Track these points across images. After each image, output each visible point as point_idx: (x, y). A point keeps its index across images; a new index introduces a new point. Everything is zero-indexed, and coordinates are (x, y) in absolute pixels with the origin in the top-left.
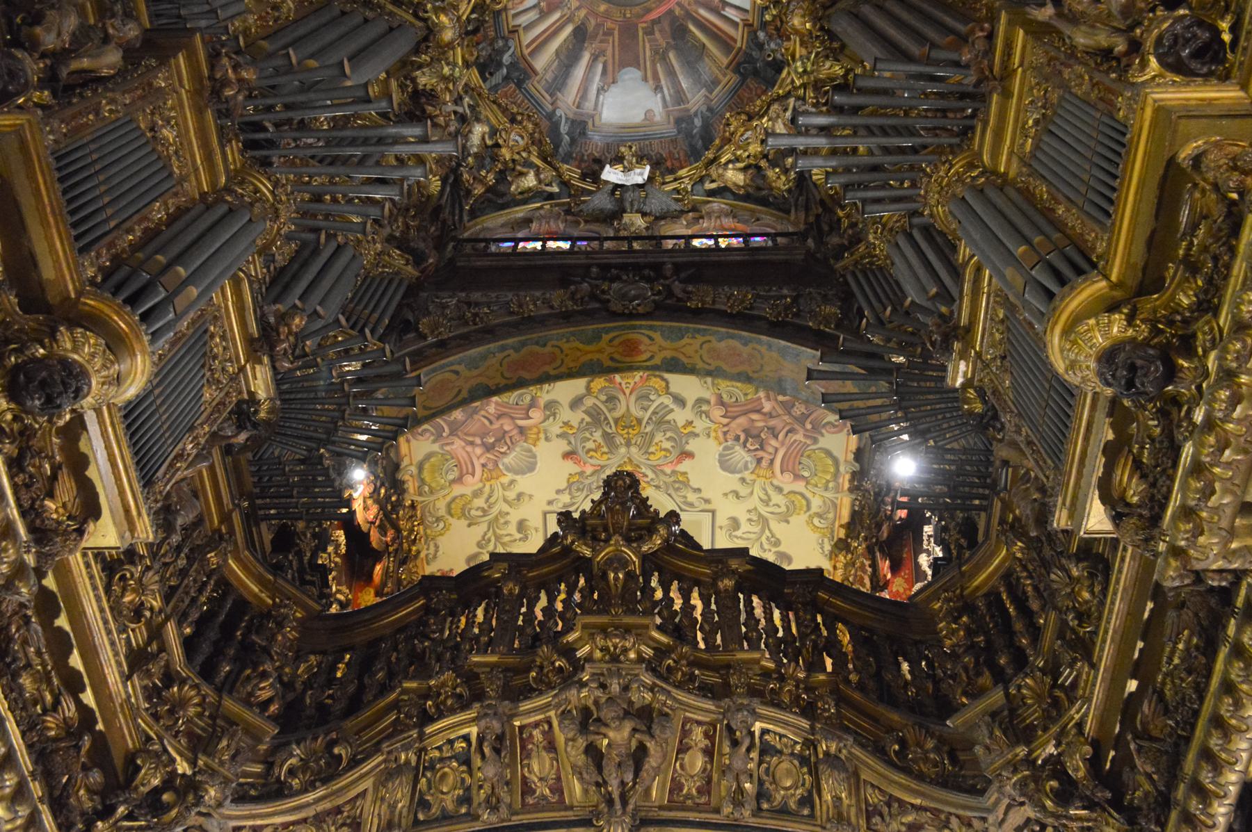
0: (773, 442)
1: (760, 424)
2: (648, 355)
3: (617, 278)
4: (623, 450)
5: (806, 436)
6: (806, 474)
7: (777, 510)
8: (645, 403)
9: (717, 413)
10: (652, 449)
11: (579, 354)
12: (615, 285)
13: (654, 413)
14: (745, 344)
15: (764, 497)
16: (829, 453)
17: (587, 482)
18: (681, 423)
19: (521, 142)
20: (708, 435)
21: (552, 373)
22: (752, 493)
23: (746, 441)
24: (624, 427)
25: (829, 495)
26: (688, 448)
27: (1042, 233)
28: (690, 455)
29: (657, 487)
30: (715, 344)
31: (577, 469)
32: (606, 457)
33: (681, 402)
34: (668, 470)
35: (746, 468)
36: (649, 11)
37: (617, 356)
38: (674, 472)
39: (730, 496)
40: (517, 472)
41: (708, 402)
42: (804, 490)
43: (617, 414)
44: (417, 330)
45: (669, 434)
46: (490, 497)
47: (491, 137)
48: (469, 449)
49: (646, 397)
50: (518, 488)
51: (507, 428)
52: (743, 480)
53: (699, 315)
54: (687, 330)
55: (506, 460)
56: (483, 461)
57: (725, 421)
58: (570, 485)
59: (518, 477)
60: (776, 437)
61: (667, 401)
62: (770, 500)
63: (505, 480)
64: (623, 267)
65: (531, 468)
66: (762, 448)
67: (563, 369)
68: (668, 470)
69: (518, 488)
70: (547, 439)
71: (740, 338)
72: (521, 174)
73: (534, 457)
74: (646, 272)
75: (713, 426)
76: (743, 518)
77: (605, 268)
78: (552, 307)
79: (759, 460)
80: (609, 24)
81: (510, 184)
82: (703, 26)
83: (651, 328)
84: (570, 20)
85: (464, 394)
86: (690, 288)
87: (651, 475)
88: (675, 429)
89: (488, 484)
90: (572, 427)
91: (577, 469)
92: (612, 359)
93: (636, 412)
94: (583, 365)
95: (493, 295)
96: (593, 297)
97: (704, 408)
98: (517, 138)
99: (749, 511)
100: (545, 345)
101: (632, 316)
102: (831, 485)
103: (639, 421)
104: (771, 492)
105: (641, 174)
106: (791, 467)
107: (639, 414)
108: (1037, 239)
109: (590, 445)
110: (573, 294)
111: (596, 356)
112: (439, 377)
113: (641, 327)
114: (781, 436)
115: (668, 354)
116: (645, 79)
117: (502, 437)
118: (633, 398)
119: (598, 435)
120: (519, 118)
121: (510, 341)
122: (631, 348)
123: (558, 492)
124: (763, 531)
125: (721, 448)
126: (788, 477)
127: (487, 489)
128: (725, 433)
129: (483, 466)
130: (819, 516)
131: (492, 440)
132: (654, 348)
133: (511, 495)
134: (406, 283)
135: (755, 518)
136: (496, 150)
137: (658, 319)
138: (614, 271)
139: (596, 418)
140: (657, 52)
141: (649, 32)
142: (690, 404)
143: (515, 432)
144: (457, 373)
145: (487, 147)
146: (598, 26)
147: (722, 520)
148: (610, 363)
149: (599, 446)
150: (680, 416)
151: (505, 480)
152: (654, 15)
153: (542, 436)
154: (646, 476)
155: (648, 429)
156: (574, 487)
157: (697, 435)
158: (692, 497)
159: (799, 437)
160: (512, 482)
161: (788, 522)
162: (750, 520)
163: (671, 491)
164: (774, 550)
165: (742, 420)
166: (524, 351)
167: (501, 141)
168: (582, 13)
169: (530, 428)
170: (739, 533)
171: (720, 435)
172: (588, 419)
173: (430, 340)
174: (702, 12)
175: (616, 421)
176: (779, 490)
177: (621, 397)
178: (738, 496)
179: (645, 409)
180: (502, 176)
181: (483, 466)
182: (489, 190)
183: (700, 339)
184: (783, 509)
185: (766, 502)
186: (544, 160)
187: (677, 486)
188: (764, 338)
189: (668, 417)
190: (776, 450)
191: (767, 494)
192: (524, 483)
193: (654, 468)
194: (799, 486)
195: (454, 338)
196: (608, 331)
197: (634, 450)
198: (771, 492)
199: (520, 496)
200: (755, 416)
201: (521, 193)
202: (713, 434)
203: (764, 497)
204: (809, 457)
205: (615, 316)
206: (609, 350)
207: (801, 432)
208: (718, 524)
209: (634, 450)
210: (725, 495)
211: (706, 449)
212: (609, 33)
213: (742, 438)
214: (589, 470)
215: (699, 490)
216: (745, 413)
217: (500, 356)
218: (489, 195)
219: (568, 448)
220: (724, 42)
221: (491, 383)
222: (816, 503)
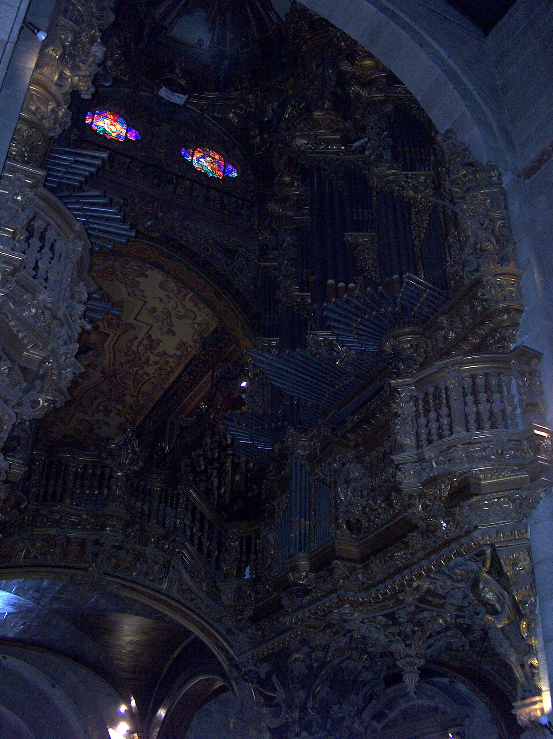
7: (178, 313)
10: (127, 267)
14: (200, 278)
22: (169, 302)
26: (146, 273)
27: (305, 518)
28: (146, 276)
29: (121, 282)
32: (100, 261)
35: (172, 291)
39: (158, 300)
68: (130, 277)
79: (180, 292)
105: (182, 99)
108: (303, 520)
116: (207, 20)
124: (167, 318)
125: (163, 279)
126: (192, 303)
130: (198, 324)
135: (165, 312)
147: (147, 306)
154: (118, 276)
158: (137, 292)
161: (181, 320)
162: (162, 312)
164: (168, 327)
170: (154, 314)
176: (184, 307)
178: (161, 300)
187: (132, 285)
194: (195, 309)
203: (175, 306)
208: (146, 306)
210: (156, 298)
215: (143, 291)
222: (199, 319)
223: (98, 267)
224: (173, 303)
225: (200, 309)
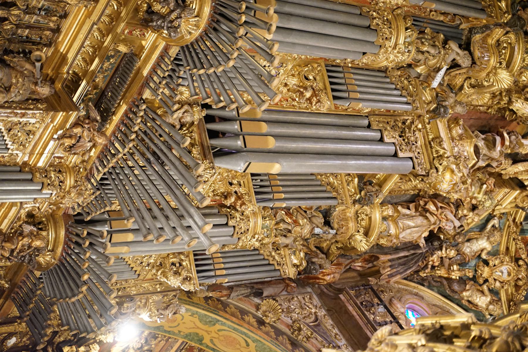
19: (505, 277)
47: (489, 253)
72: (482, 292)
81: (465, 290)
95: (336, 331)
98: (505, 272)
112: (234, 335)
120: (521, 263)
134: (278, 274)
136: (481, 264)
144: (248, 345)
145: (479, 256)
167: (491, 263)
173: (259, 314)
180: (462, 281)
182: (449, 279)
186: (509, 301)
201: (469, 302)
218: (445, 283)
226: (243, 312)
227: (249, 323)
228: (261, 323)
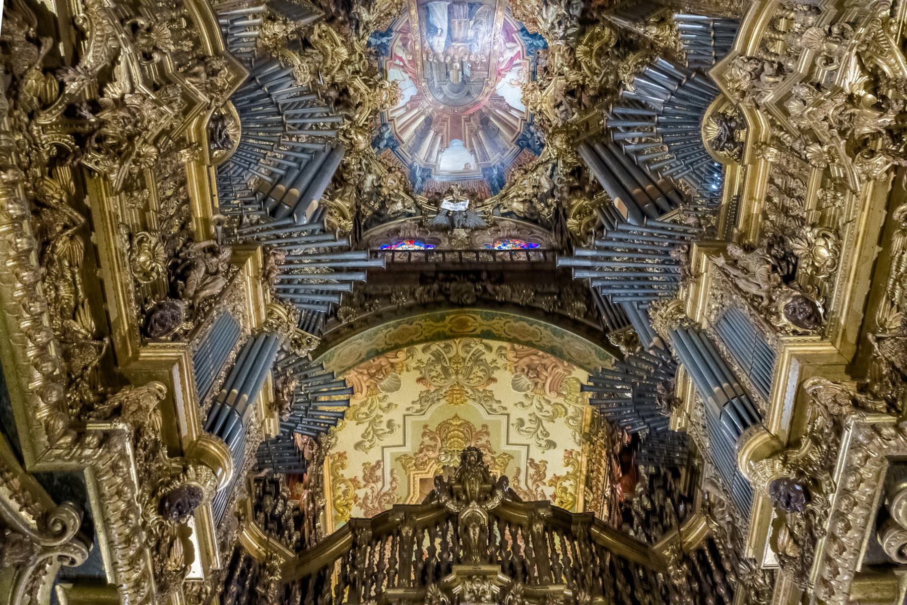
0: (545, 373)
1: (537, 362)
2: (472, 328)
3: (455, 280)
4: (454, 377)
5: (565, 370)
6: (565, 393)
8: (468, 349)
9: (511, 355)
10: (471, 377)
11: (431, 328)
12: (453, 285)
13: (473, 354)
14: (531, 325)
15: (539, 406)
16: (578, 380)
17: (431, 396)
18: (489, 361)
20: (506, 368)
21: (415, 340)
23: (528, 372)
24: (455, 363)
25: (579, 406)
26: (493, 376)
28: (494, 380)
30: (513, 323)
31: (424, 388)
33: (489, 348)
34: (481, 390)
35: (528, 389)
36: (468, 109)
37: (454, 329)
38: (484, 390)
40: (388, 390)
41: (506, 349)
42: (563, 403)
43: (450, 355)
44: (336, 316)
45: (482, 367)
46: (371, 406)
48: (360, 377)
49: (468, 345)
50: (388, 401)
51: (383, 364)
52: (526, 396)
53: (502, 305)
54: (496, 315)
55: (382, 383)
56: (367, 384)
57: (516, 360)
58: (421, 398)
59: (389, 394)
60: (546, 370)
61: (481, 348)
62: (543, 407)
63: (381, 396)
64: (457, 272)
65: (397, 388)
66: (538, 377)
67: (422, 337)
68: (481, 390)
69: (388, 401)
70: (408, 370)
71: (527, 321)
73: (400, 381)
74: (471, 276)
75: (509, 363)
76: (526, 418)
77: (447, 272)
78: (415, 299)
79: (536, 384)
80: (445, 116)
82: (498, 119)
83: (475, 313)
84: (422, 114)
85: (363, 356)
86: (498, 288)
87: (470, 392)
88: (486, 364)
89: (370, 398)
90: (423, 363)
91: (424, 388)
92: (451, 330)
93: (462, 354)
94: (434, 334)
96: (440, 291)
97: (503, 352)
99: (530, 415)
100: (411, 324)
101: (462, 305)
102: (580, 400)
103: (464, 359)
104: (543, 403)
106: (556, 388)
107: (464, 355)
109: (434, 374)
110: (429, 292)
111: (441, 329)
113: (469, 312)
114: (549, 370)
115: (485, 328)
117: (380, 369)
118: (460, 346)
119: (438, 368)
121: (392, 322)
122: (463, 324)
123: (413, 402)
126: (554, 394)
127: (370, 401)
128: (516, 367)
129: (368, 387)
131: (374, 371)
132: (476, 324)
133: (384, 405)
137: (480, 307)
138: (452, 276)
139: (438, 357)
140: (472, 131)
141: (468, 120)
142: (495, 350)
143: (388, 366)
144: (359, 344)
146: (438, 116)
148: (450, 333)
149: (439, 374)
150: (489, 357)
151: (381, 396)
152: (471, 112)
153: (405, 368)
155: (469, 365)
156: (423, 400)
157: (499, 368)
158: (495, 406)
159: (560, 370)
160: (385, 397)
163: (483, 402)
165: (526, 360)
166: (400, 327)
168: (430, 110)
169: (397, 364)
171: (513, 368)
172: (433, 358)
173: (344, 323)
174: (498, 111)
175: (450, 359)
176: (549, 402)
177: (453, 345)
178: (523, 406)
179: (468, 352)
181: (368, 387)
183: (504, 320)
184: (551, 414)
185: (541, 409)
188: (543, 322)
189: (482, 357)
190: (547, 378)
191: (540, 404)
192: (393, 397)
193: (472, 388)
194: (560, 400)
195: (358, 321)
196: (448, 314)
197: (460, 377)
198: (543, 403)
199: (389, 405)
200: (534, 357)
202: (508, 368)
203: (539, 406)
204: (566, 382)
205: (453, 305)
206: (449, 325)
207: (561, 367)
209: (460, 377)
210: (516, 405)
211: (504, 377)
212: (445, 120)
213: (526, 370)
214: (432, 389)
215: (499, 402)
216: (528, 355)
217: (385, 331)
219: (420, 376)
220: (511, 129)
221: (379, 348)
223: (444, 390)
224: (535, 402)
225: (566, 398)
226: (337, 332)
227: (347, 333)
228: (351, 326)
